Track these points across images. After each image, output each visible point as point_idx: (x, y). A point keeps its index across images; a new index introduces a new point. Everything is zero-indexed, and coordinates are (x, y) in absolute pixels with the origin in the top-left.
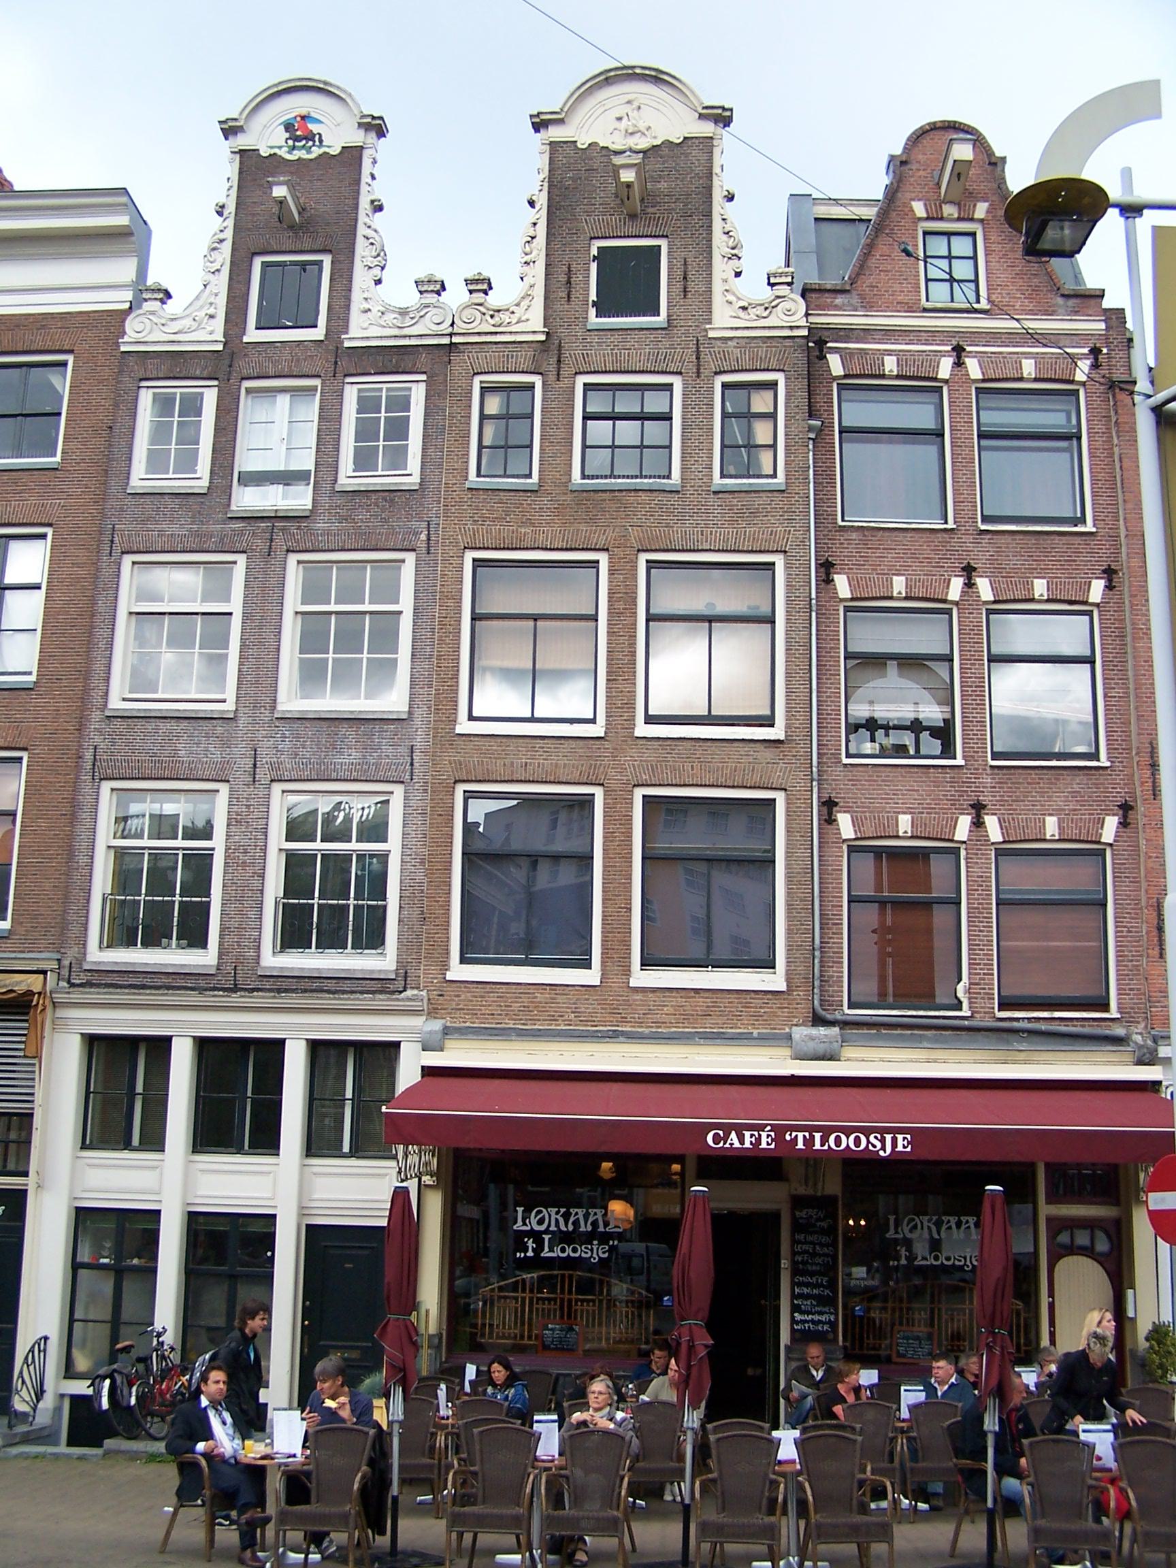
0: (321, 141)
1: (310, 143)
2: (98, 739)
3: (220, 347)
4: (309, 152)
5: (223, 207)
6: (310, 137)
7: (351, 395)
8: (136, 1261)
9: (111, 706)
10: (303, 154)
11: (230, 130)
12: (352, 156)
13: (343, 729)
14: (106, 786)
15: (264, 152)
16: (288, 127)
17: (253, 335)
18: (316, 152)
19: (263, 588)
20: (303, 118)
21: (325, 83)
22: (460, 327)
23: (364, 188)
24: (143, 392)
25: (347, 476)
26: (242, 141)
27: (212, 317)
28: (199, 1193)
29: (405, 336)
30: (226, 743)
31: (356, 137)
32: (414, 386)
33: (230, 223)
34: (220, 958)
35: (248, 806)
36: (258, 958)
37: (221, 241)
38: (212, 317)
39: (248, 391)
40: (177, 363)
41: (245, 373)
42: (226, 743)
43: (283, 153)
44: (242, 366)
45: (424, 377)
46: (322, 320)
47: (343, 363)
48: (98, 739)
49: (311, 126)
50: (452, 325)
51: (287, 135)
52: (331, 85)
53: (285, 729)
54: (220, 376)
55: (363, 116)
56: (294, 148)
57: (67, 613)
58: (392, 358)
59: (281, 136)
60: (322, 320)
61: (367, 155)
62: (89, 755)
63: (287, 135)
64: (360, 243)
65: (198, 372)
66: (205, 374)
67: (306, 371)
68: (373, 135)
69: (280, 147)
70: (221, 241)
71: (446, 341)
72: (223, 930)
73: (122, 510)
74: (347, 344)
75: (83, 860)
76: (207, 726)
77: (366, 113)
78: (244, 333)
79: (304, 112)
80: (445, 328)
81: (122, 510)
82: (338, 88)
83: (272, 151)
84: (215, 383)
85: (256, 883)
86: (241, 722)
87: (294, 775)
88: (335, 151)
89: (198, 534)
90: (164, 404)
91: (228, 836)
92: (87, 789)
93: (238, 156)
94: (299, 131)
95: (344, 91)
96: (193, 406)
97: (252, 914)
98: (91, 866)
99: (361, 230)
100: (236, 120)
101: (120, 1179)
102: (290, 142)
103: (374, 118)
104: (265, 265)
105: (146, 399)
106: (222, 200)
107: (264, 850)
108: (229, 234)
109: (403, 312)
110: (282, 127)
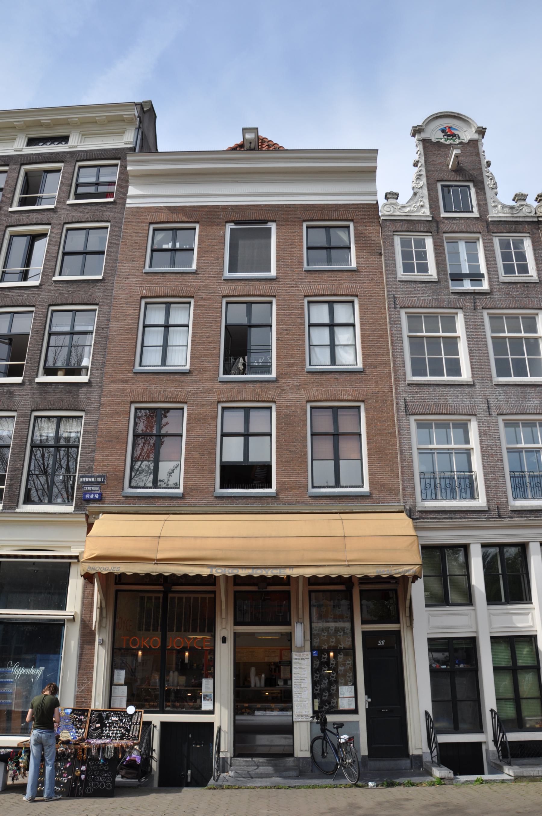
0: (459, 137)
1: (454, 138)
2: (405, 395)
3: (430, 219)
4: (454, 141)
5: (418, 162)
6: (453, 135)
7: (496, 241)
8: (462, 666)
9: (407, 379)
10: (451, 141)
11: (417, 131)
12: (474, 144)
13: (529, 390)
14: (412, 419)
15: (434, 140)
16: (443, 131)
17: (443, 215)
18: (457, 141)
19: (475, 325)
20: (449, 128)
21: (458, 114)
22: (539, 214)
23: (482, 157)
24: (395, 237)
25: (503, 277)
26: (423, 136)
27: (422, 206)
28: (494, 626)
29: (517, 217)
30: (471, 396)
31: (476, 136)
32: (524, 239)
33: (423, 169)
34: (488, 501)
35: (489, 427)
36: (507, 502)
37: (420, 175)
38: (422, 206)
39: (446, 238)
40: (410, 225)
41: (445, 229)
42: (471, 396)
43: (442, 141)
44: (444, 227)
45: (528, 235)
46: (475, 209)
47: (491, 227)
48: (405, 395)
49: (453, 131)
50: (536, 213)
51: (443, 134)
52: (461, 115)
53: (500, 389)
54: (433, 230)
55: (478, 127)
56: (448, 139)
57: (374, 336)
58: (514, 225)
59: (440, 135)
60: (475, 209)
61: (479, 143)
62: (402, 403)
63: (443, 134)
64: (485, 179)
65: (422, 229)
66: (425, 230)
67: (473, 230)
68: (481, 136)
69: (441, 139)
70: (420, 175)
71: (536, 219)
72: (488, 488)
73: (396, 288)
74: (490, 219)
75: (407, 455)
76: (460, 389)
77: (480, 125)
78: (440, 214)
79: (449, 125)
80: (533, 214)
81: (396, 288)
82: (465, 116)
83: (438, 140)
84: (430, 234)
85: (499, 463)
86: (478, 386)
87: (508, 411)
88: (466, 140)
89: (437, 300)
90: (405, 243)
91: (481, 442)
92: (404, 419)
93: (421, 142)
94: (448, 133)
95: (468, 118)
96: (421, 244)
97: (501, 480)
98: (411, 457)
99: (485, 174)
100: (421, 126)
101: (452, 622)
102: (446, 137)
103: (483, 129)
104: (442, 186)
105: (397, 240)
106: (417, 158)
107: (500, 448)
108: (424, 173)
109: (512, 208)
110: (440, 131)
